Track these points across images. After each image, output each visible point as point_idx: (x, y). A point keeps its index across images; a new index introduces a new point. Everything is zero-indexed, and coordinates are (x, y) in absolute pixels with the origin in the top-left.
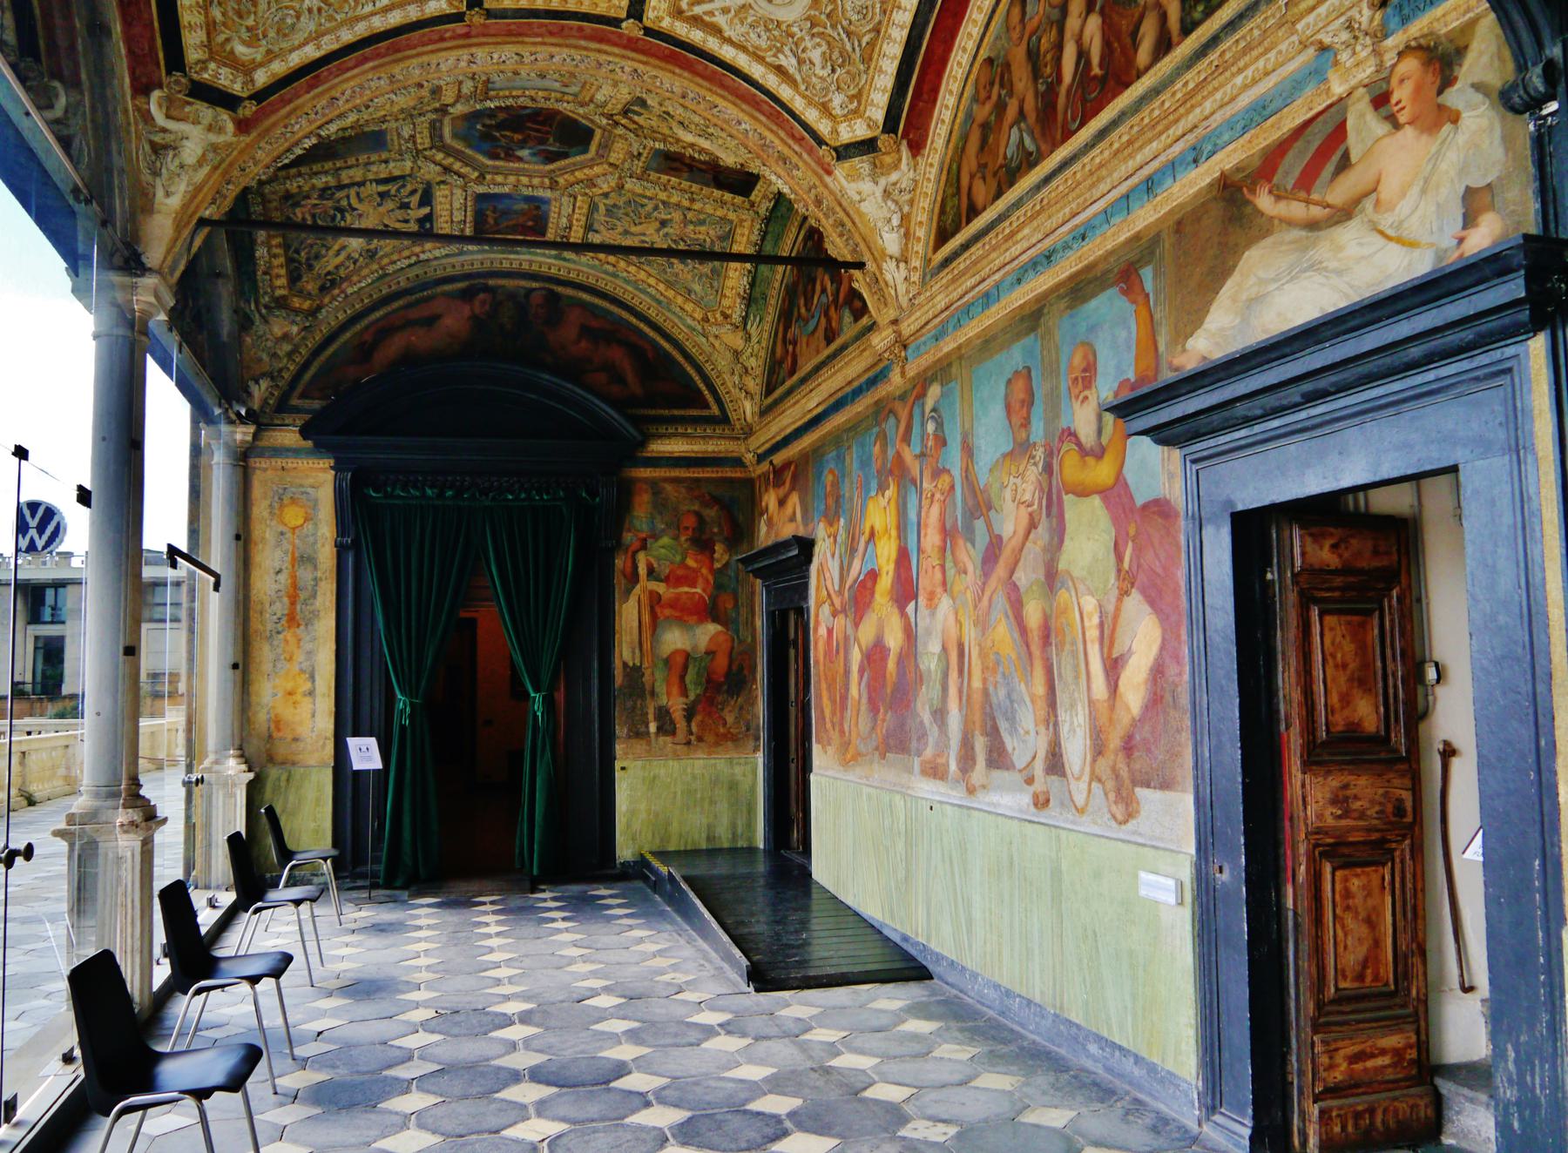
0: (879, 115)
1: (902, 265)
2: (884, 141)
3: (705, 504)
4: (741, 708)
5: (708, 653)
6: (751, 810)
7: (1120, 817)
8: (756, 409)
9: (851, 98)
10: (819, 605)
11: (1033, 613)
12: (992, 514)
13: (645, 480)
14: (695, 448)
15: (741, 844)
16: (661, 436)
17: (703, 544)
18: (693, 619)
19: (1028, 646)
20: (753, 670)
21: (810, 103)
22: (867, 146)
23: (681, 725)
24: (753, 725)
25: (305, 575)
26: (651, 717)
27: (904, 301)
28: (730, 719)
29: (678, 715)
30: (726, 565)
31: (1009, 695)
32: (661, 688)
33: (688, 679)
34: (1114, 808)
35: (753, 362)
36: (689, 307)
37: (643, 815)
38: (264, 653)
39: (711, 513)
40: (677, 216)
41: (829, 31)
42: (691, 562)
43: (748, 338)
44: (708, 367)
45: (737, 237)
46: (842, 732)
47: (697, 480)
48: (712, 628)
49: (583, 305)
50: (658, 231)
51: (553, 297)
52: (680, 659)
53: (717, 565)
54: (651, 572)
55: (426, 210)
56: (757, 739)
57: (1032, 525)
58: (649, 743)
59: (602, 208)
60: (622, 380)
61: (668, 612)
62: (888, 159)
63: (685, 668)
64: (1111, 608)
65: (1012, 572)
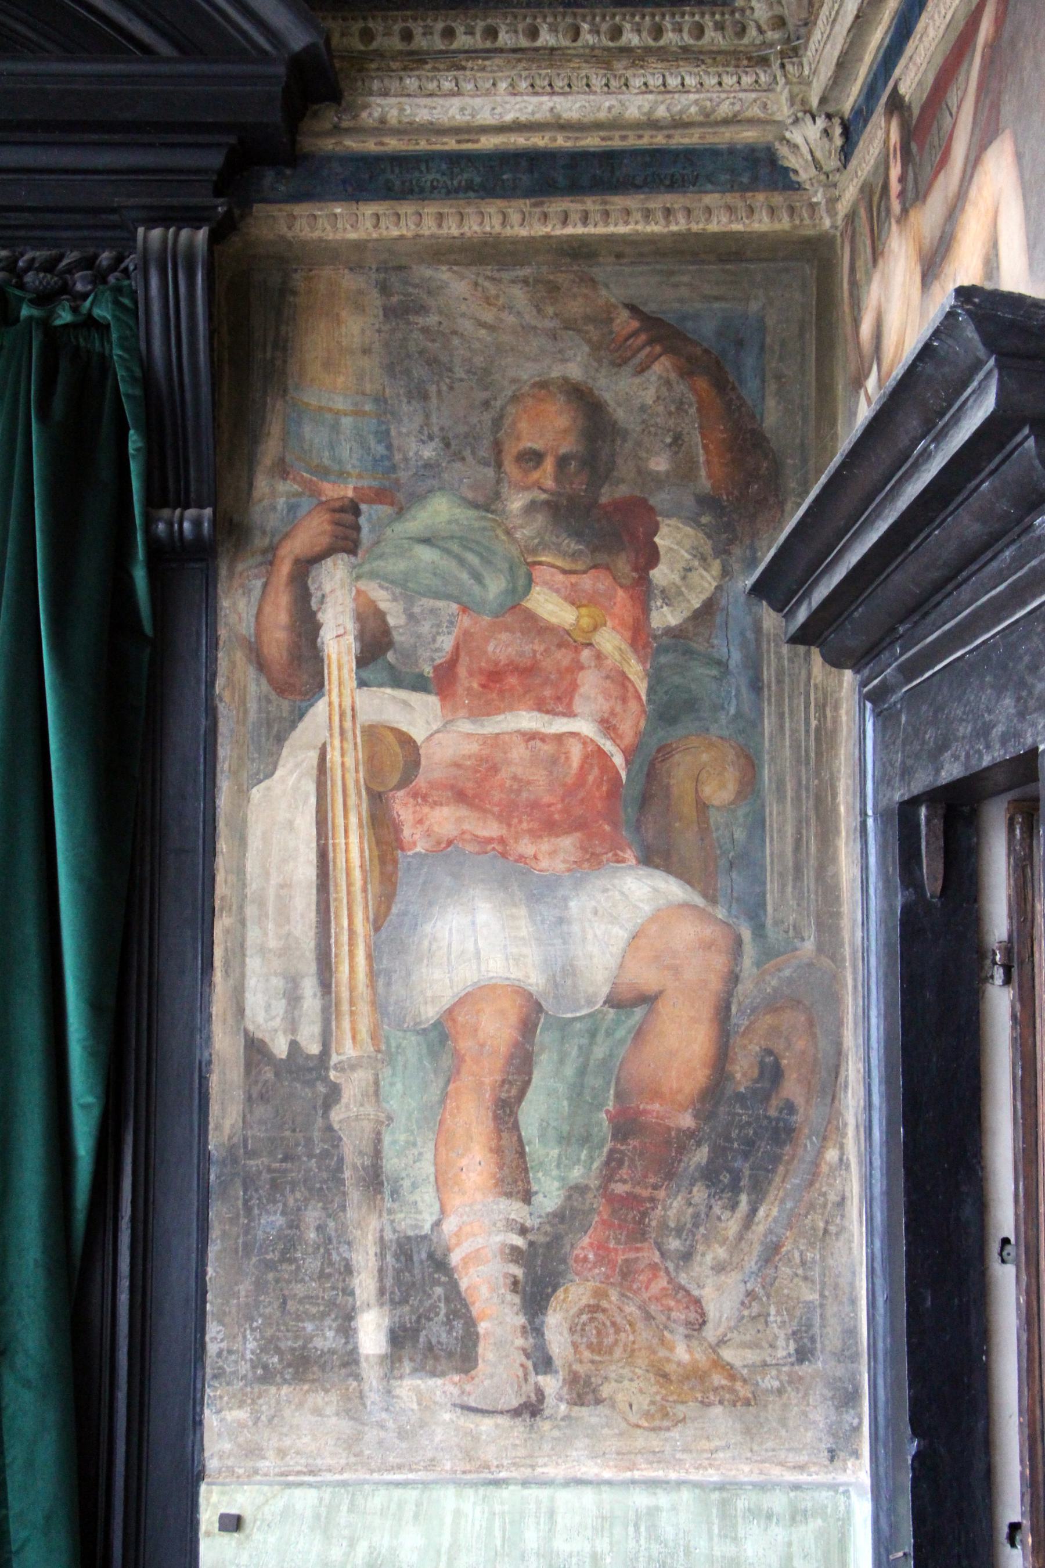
3: (616, 354)
4: (772, 1252)
5: (614, 1001)
13: (354, 256)
14: (572, 107)
16: (416, 60)
17: (604, 525)
20: (828, 1082)
23: (497, 1317)
24: (831, 1338)
26: (365, 1284)
28: (721, 1299)
29: (484, 1277)
30: (709, 608)
32: (410, 1159)
33: (534, 1113)
39: (639, 392)
42: (549, 605)
47: (579, 252)
48: (640, 892)
52: (496, 1029)
53: (665, 617)
54: (375, 648)
58: (353, 1407)
61: (446, 819)
63: (521, 1065)
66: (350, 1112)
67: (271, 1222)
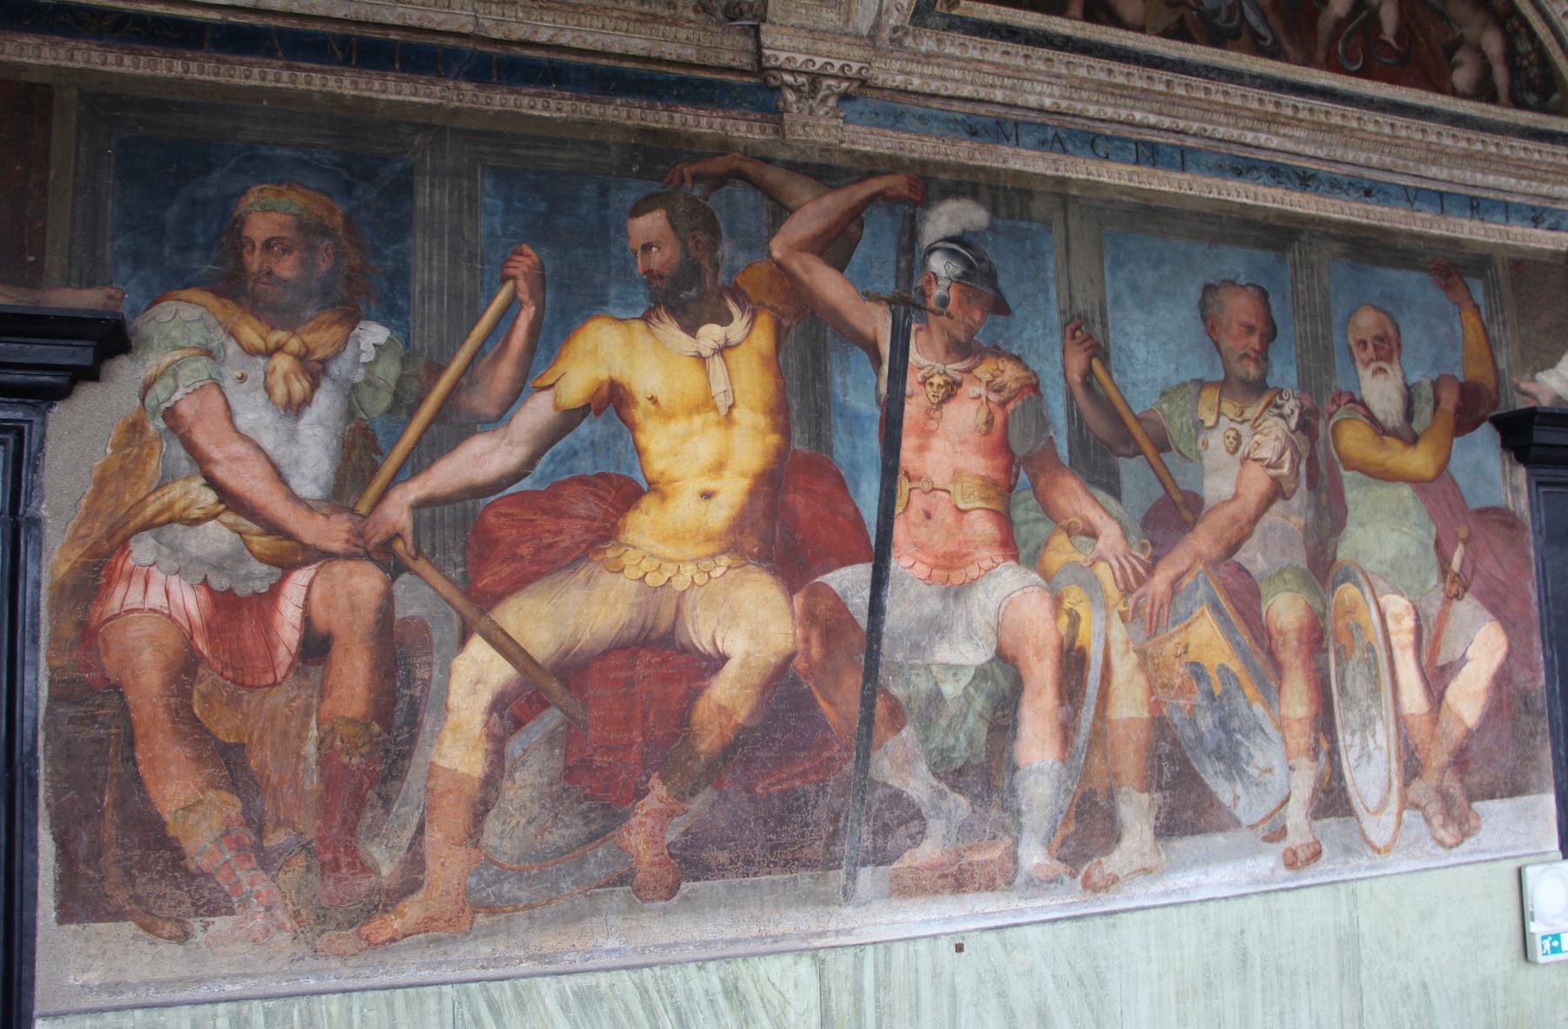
7: (1449, 840)
11: (1285, 610)
19: (1271, 653)
31: (1222, 723)
34: (1441, 833)
57: (1277, 492)
64: (1434, 610)
65: (1233, 549)
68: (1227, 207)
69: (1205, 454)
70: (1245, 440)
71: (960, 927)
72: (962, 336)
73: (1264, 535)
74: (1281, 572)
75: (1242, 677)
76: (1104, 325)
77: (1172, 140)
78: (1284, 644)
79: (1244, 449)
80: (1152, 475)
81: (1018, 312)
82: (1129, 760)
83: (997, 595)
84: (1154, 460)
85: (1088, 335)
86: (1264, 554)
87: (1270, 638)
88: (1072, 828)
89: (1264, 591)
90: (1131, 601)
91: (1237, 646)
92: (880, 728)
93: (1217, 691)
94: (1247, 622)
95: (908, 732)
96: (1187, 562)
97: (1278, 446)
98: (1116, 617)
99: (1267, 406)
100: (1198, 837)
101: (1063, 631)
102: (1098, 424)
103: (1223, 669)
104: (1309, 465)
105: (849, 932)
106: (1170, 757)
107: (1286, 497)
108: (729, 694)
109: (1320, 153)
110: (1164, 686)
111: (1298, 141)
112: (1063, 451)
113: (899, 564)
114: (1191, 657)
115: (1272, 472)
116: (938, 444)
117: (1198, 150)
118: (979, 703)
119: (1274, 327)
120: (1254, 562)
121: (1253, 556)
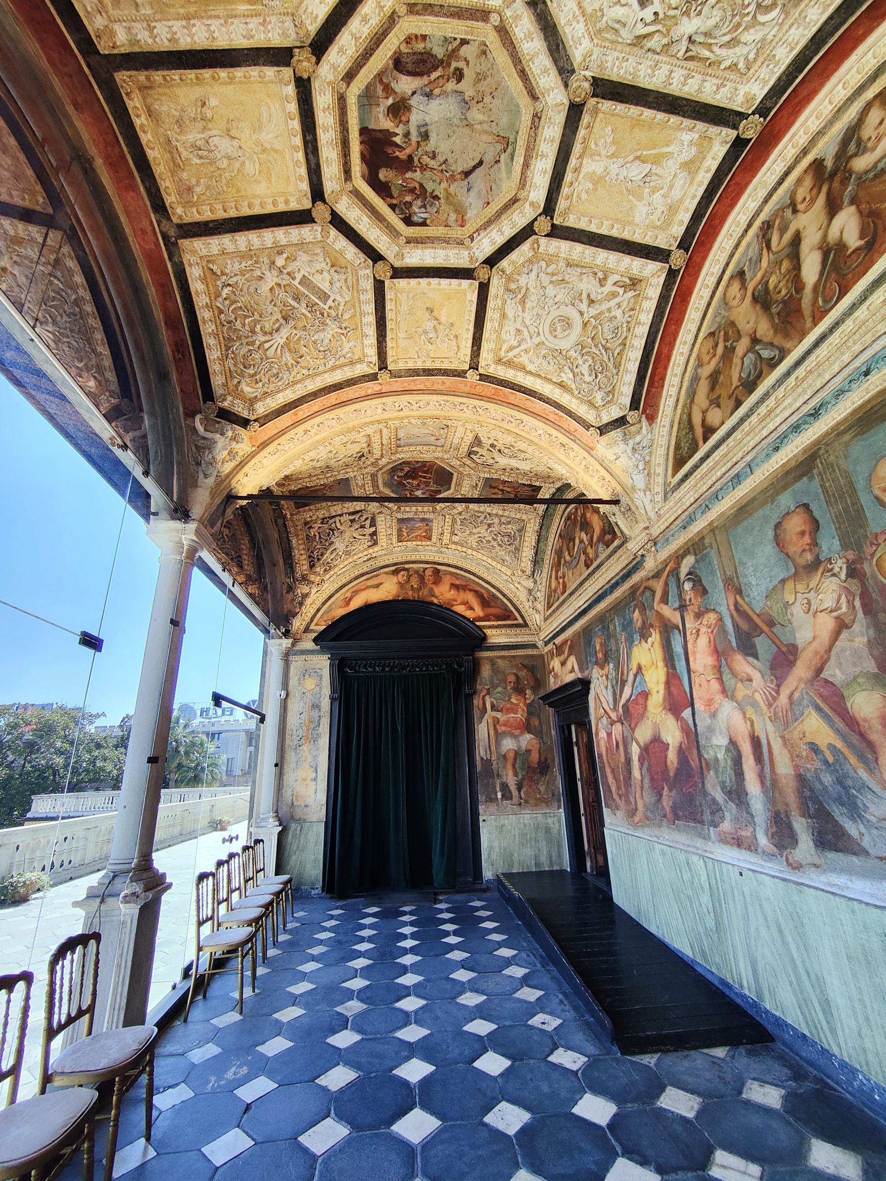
0: (627, 401)
1: (648, 493)
2: (632, 416)
4: (548, 783)
6: (560, 846)
8: (542, 618)
9: (608, 393)
10: (599, 719)
12: (777, 629)
14: (512, 640)
15: (556, 868)
17: (519, 690)
18: (517, 732)
20: (553, 760)
21: (582, 401)
22: (621, 422)
23: (515, 793)
24: (556, 793)
25: (315, 714)
26: (498, 789)
27: (652, 515)
28: (542, 789)
29: (513, 788)
31: (840, 781)
33: (517, 766)
35: (539, 594)
36: (504, 569)
37: (497, 850)
38: (290, 756)
39: (523, 673)
40: (496, 521)
41: (594, 350)
42: (514, 700)
43: (535, 582)
44: (515, 600)
45: (528, 529)
46: (628, 802)
47: (514, 657)
48: (528, 736)
49: (451, 574)
50: (487, 530)
51: (437, 571)
52: (512, 755)
53: (528, 702)
54: (493, 708)
55: (373, 529)
56: (560, 801)
57: (842, 625)
59: (459, 522)
60: (472, 609)
61: (503, 728)
62: (633, 429)
65: (819, 671)
66: (494, 766)
67: (485, 781)
68: (775, 475)
69: (793, 620)
70: (813, 603)
71: (744, 865)
72: (697, 610)
73: (838, 656)
74: (855, 678)
75: (846, 751)
76: (738, 577)
77: (741, 465)
78: (870, 728)
79: (813, 607)
80: (770, 642)
81: (709, 590)
82: (792, 798)
83: (725, 714)
84: (769, 634)
85: (735, 587)
86: (840, 669)
87: (858, 724)
88: (774, 829)
89: (846, 694)
90: (772, 710)
91: (837, 731)
92: (705, 771)
93: (831, 760)
94: (840, 716)
95: (712, 773)
96: (795, 684)
97: (835, 595)
98: (767, 720)
99: (822, 574)
100: (840, 854)
101: (749, 728)
102: (744, 626)
103: (831, 747)
104: (862, 598)
105: (712, 853)
106: (811, 798)
107: (848, 627)
108: (672, 756)
109: (807, 397)
110: (798, 756)
111: (790, 405)
112: (734, 644)
113: (696, 706)
114: (808, 739)
115: (834, 614)
116: (698, 656)
117: (755, 457)
118: (729, 762)
119: (817, 522)
120: (834, 676)
121: (834, 673)
